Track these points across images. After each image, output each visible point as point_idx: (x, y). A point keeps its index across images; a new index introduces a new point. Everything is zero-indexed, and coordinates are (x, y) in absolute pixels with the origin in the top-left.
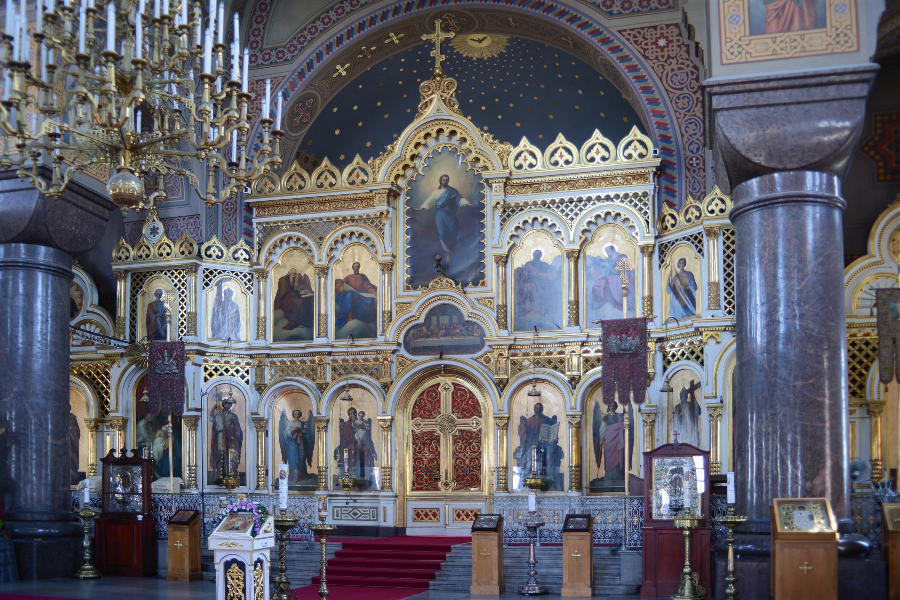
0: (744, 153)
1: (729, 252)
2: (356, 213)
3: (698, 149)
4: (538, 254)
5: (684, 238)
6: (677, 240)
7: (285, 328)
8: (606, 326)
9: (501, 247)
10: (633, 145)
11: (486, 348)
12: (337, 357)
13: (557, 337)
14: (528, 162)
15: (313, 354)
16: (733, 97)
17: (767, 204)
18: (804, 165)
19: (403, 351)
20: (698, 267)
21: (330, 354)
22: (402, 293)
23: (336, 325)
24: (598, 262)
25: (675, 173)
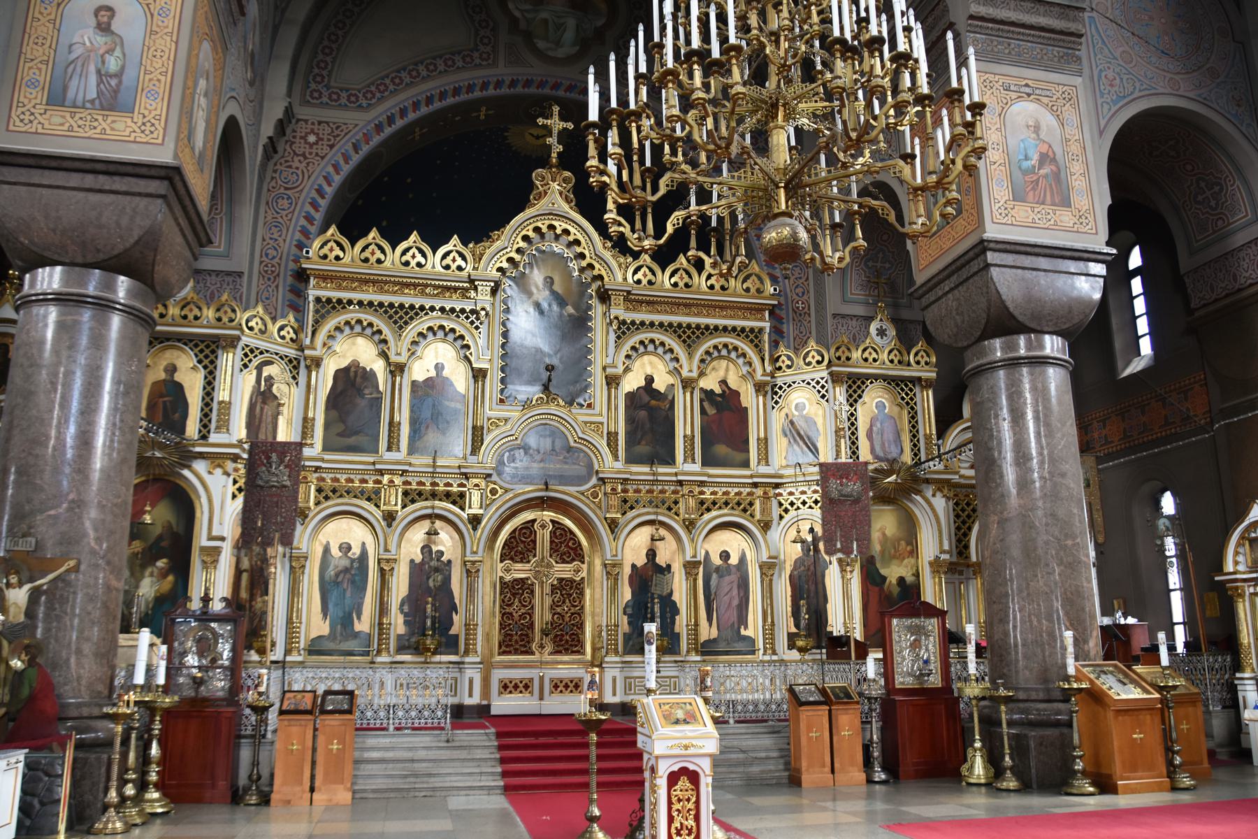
0: (1011, 310)
3: (803, 293)
4: (649, 380)
5: (803, 381)
6: (794, 383)
7: (340, 435)
8: (824, 469)
9: (616, 367)
10: (751, 279)
11: (594, 481)
13: (676, 474)
14: (648, 278)
16: (1004, 255)
17: (1013, 363)
18: (1057, 329)
20: (820, 412)
24: (708, 395)
25: (783, 313)
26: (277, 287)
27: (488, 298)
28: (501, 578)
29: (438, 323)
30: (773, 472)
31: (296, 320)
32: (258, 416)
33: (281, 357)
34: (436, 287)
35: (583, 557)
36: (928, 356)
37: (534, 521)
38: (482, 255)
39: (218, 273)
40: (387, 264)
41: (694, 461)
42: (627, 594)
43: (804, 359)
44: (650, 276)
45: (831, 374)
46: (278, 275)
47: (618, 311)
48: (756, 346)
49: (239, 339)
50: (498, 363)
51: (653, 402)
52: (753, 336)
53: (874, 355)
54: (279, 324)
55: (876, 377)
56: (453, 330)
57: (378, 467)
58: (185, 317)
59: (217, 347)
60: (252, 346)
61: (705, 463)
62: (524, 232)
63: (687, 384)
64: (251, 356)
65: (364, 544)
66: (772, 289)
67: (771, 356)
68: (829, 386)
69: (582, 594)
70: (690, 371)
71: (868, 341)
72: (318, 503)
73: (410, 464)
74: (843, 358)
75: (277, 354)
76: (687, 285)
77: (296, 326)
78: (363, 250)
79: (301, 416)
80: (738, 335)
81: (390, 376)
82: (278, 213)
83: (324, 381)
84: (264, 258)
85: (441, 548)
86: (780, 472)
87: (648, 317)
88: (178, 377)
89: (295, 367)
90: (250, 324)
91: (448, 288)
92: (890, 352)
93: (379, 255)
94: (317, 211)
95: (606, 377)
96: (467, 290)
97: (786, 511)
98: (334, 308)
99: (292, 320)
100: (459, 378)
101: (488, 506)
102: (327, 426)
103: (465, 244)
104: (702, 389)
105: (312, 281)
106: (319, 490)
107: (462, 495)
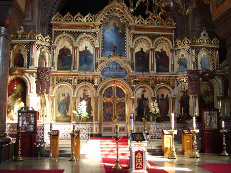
1: (196, 54)
2: (88, 31)
4: (142, 49)
5: (183, 49)
6: (181, 49)
7: (62, 66)
11: (127, 76)
12: (79, 77)
15: (72, 75)
19: (101, 76)
20: (188, 57)
21: (78, 75)
22: (101, 57)
23: (79, 66)
24: (158, 53)
26: (45, 29)
27: (98, 29)
28: (104, 102)
29: (85, 35)
30: (175, 73)
31: (50, 37)
32: (41, 62)
33: (46, 47)
34: (85, 27)
35: (125, 96)
36: (217, 41)
37: (112, 87)
38: (96, 17)
39: (30, 26)
40: (72, 20)
41: (154, 71)
42: (136, 106)
43: (184, 43)
44: (141, 21)
45: (191, 47)
46: (45, 25)
47: (133, 31)
48: (170, 40)
49: (35, 42)
50: (101, 46)
51: (143, 55)
52: (169, 37)
53: (202, 41)
54: (45, 38)
55: (203, 47)
56: (89, 38)
57: (71, 74)
58: (22, 37)
59: (30, 45)
60: (39, 44)
61: (157, 71)
62: (108, 11)
63: (152, 50)
64: (39, 46)
65: (68, 94)
66: (174, 24)
67: (174, 42)
68: (190, 50)
69: (125, 106)
70: (153, 46)
71: (200, 38)
72: (57, 83)
73: (79, 73)
74: (194, 42)
75: (45, 46)
76: (151, 24)
77: (50, 38)
78: (66, 18)
79: (52, 61)
80: (166, 37)
81: (73, 50)
82: (44, 10)
83: (57, 52)
84: (41, 21)
85: (88, 94)
86: (177, 73)
87: (141, 32)
88: (23, 53)
89: (50, 49)
90: (38, 38)
91: (88, 27)
92: (207, 41)
93: (70, 19)
94: (54, 8)
95: (130, 48)
96: (93, 27)
97: (179, 83)
98: (59, 33)
99: (49, 37)
100: (91, 50)
101: (99, 83)
102: (58, 64)
103: (92, 15)
104: (156, 51)
105: (53, 27)
106: (57, 80)
107: (93, 81)
